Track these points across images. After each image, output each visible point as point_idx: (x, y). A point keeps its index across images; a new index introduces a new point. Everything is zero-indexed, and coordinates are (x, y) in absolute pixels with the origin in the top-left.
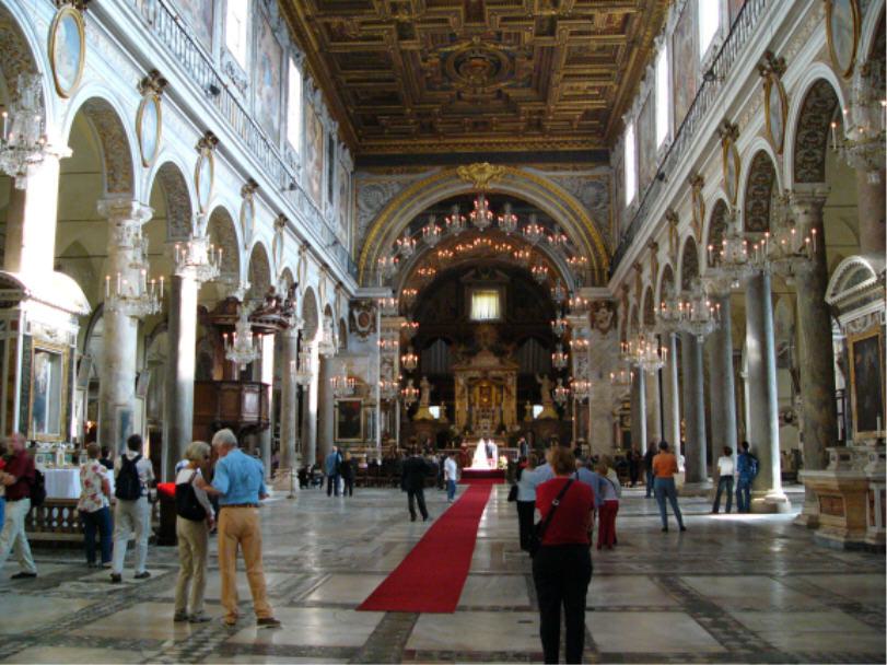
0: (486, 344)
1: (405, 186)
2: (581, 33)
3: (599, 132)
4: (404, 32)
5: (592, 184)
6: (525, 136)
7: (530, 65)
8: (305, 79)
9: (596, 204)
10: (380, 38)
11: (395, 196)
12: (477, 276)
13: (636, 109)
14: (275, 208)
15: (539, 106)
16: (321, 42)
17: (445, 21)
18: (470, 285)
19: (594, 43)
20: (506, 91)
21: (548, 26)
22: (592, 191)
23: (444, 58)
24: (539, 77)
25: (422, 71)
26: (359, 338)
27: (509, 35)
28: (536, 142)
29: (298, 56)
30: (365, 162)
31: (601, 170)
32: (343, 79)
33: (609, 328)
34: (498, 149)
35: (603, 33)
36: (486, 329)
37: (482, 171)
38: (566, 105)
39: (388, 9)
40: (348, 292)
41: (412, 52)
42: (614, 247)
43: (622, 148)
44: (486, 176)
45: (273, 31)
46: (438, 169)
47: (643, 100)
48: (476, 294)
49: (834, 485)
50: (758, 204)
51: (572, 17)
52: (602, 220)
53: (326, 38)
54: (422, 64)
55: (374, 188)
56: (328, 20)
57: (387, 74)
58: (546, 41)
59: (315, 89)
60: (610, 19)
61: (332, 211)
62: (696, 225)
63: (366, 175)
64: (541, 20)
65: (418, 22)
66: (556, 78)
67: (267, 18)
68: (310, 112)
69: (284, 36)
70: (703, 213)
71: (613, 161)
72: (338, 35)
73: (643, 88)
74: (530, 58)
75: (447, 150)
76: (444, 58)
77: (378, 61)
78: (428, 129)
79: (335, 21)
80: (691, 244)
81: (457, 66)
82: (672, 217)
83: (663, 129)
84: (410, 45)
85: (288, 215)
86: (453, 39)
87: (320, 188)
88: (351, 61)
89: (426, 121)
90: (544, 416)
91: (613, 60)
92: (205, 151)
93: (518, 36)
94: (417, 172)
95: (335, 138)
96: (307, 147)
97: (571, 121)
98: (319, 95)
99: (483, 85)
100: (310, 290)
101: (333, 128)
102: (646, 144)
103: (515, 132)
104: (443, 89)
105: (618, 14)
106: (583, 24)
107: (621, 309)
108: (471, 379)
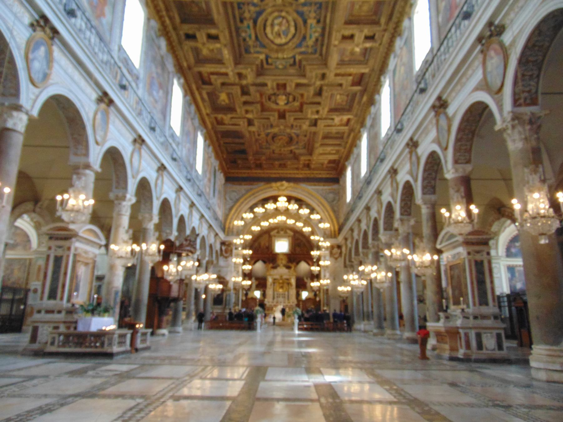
0: (282, 263)
1: (247, 191)
2: (329, 126)
3: (335, 169)
4: (250, 123)
5: (330, 193)
6: (302, 170)
7: (306, 139)
8: (205, 141)
9: (333, 201)
10: (239, 125)
11: (243, 195)
12: (278, 232)
13: (352, 159)
14: (189, 198)
15: (308, 158)
16: (212, 124)
17: (268, 119)
18: (275, 236)
19: (334, 130)
20: (294, 151)
21: (315, 123)
22: (331, 196)
23: (267, 135)
24: (309, 145)
25: (257, 140)
26: (224, 259)
27: (296, 126)
28: (305, 173)
29: (202, 131)
30: (229, 179)
31: (335, 187)
32: (222, 142)
33: (338, 257)
34: (289, 176)
35: (338, 126)
36: (281, 257)
37: (282, 185)
38: (321, 157)
39: (243, 112)
40: (220, 238)
41: (254, 132)
42: (341, 220)
43: (345, 177)
44: (284, 188)
45: (192, 119)
46: (262, 184)
47: (355, 156)
48: (278, 241)
49: (443, 330)
50: (406, 204)
51: (325, 119)
52: (336, 208)
53: (215, 123)
54: (257, 137)
55: (234, 191)
56: (216, 115)
57: (241, 141)
58: (313, 129)
59: (209, 146)
60: (341, 120)
61: (215, 201)
62: (379, 212)
63: (229, 185)
64: (311, 120)
65: (256, 118)
66: (317, 145)
67: (189, 113)
68: (207, 156)
69: (197, 122)
70: (382, 207)
71: (341, 182)
72: (220, 122)
73: (355, 150)
74: (305, 136)
75: (267, 176)
76: (267, 135)
77: (237, 135)
78: (259, 166)
79: (220, 116)
80: (376, 221)
81: (273, 138)
82: (368, 208)
83: (364, 170)
84: (252, 129)
85: (195, 202)
86: (272, 126)
87: (210, 190)
88: (227, 134)
89: (258, 162)
90: (308, 298)
91: (342, 138)
92: (160, 172)
93: (300, 127)
94: (252, 185)
95: (217, 168)
96: (204, 171)
97: (322, 164)
98: (211, 149)
99: (284, 147)
100: (203, 237)
101: (216, 163)
102: (356, 175)
103: (297, 169)
104: (267, 148)
105: (345, 118)
106: (329, 122)
107: (344, 249)
108: (275, 279)
